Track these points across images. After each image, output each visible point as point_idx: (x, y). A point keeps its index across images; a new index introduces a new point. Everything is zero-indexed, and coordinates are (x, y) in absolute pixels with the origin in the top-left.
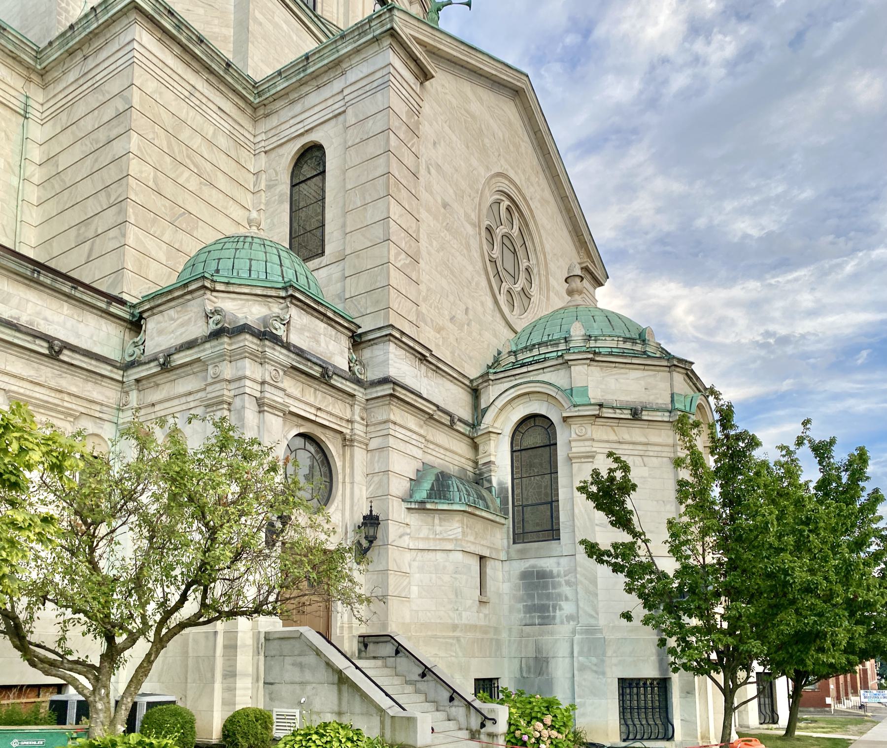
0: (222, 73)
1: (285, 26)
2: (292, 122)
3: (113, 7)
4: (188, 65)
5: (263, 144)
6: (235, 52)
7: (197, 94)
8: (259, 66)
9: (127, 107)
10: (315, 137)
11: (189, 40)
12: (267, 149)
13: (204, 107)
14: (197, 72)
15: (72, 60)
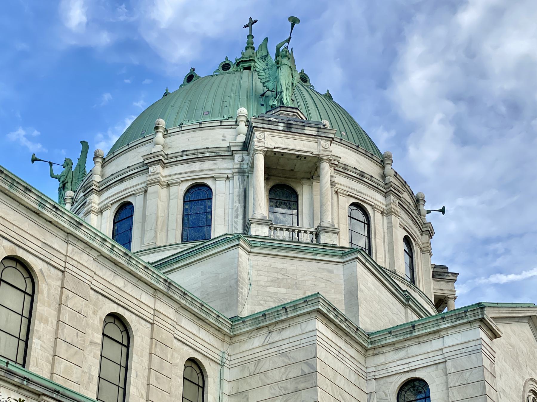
0: (354, 335)
1: (372, 287)
2: (398, 363)
3: (301, 310)
4: (337, 334)
5: (373, 374)
6: (346, 310)
7: (342, 352)
8: (367, 321)
9: (312, 371)
10: (418, 374)
11: (340, 322)
12: (376, 377)
13: (344, 359)
14: (340, 337)
15: (258, 332)
